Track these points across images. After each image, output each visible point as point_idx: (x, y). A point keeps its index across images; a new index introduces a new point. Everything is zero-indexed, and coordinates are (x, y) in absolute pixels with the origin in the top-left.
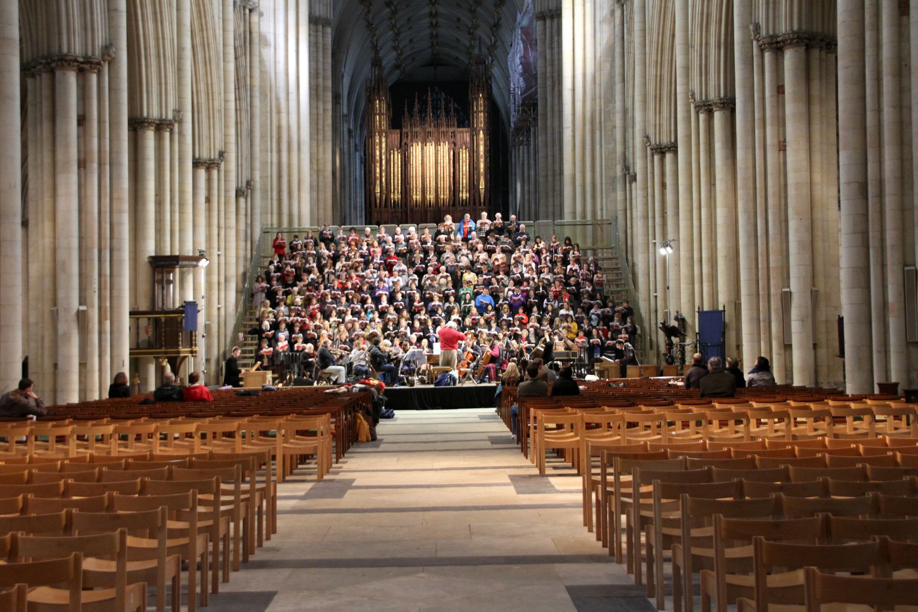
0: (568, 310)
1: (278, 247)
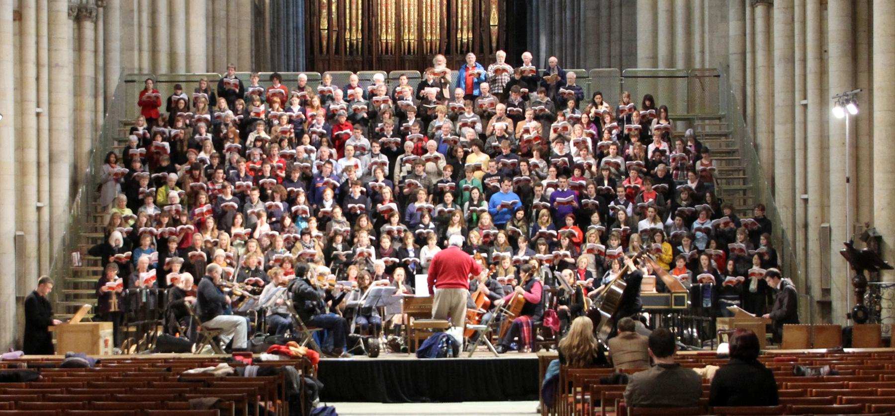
0: (654, 220)
1: (148, 106)
